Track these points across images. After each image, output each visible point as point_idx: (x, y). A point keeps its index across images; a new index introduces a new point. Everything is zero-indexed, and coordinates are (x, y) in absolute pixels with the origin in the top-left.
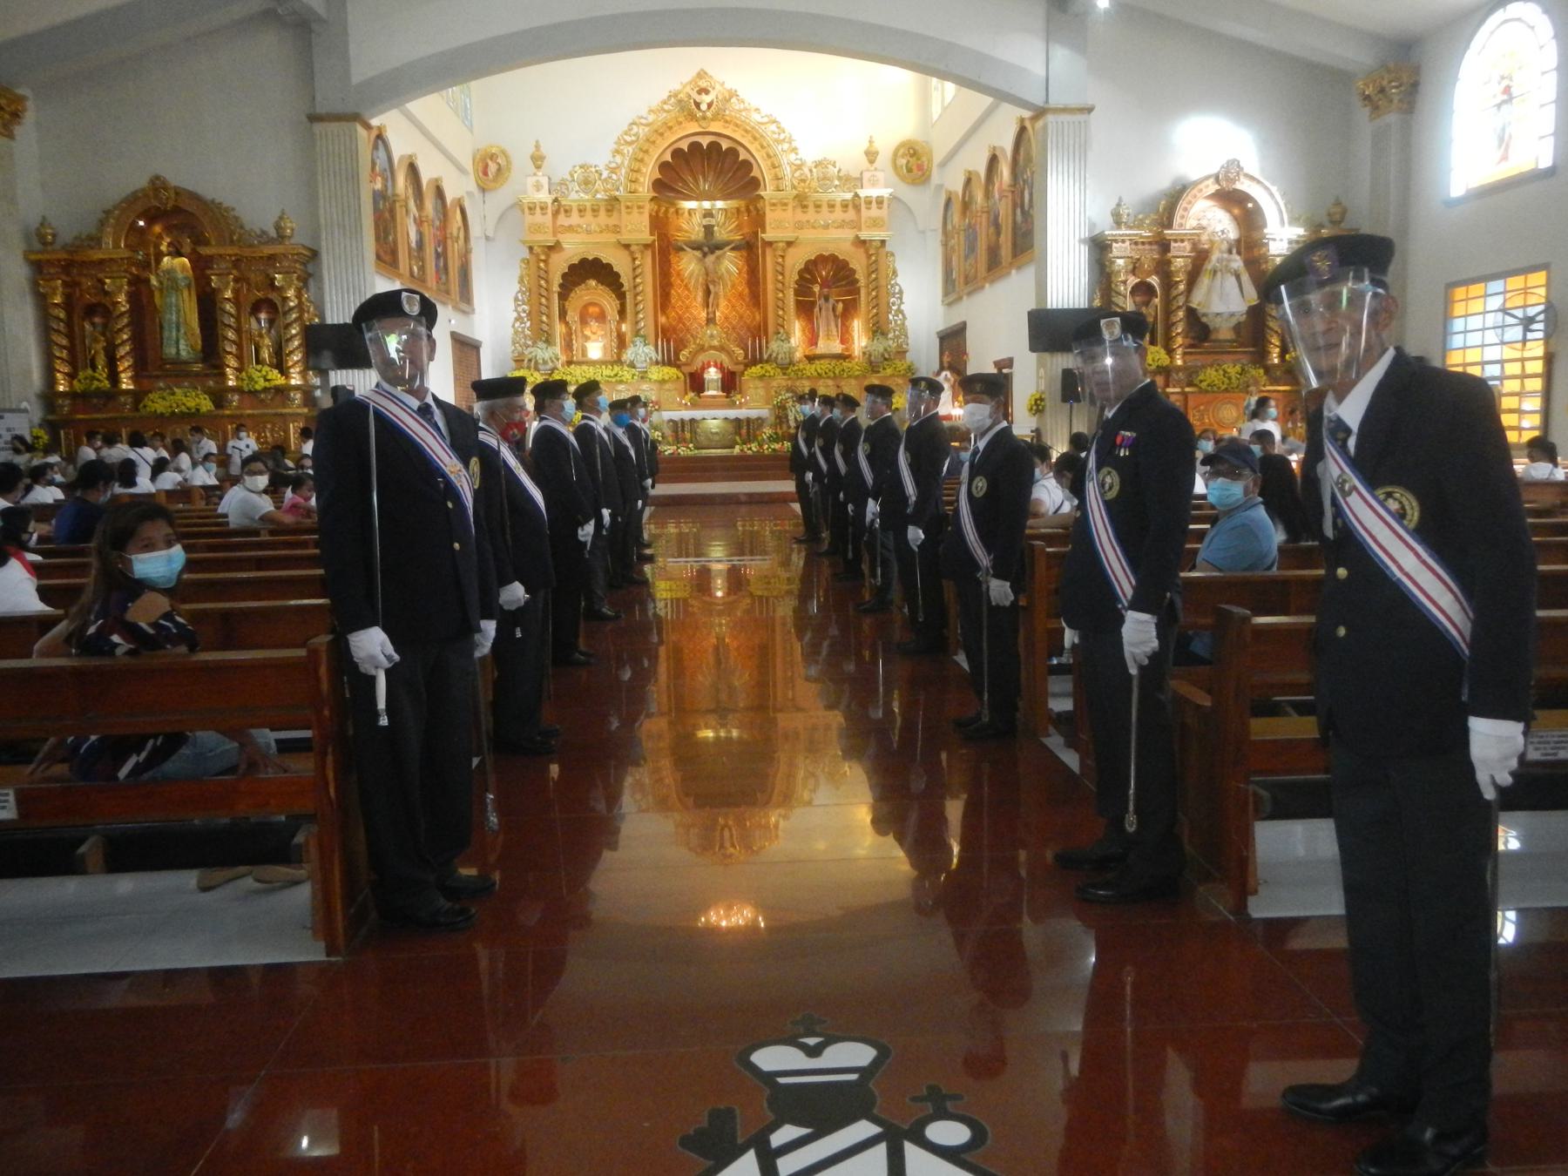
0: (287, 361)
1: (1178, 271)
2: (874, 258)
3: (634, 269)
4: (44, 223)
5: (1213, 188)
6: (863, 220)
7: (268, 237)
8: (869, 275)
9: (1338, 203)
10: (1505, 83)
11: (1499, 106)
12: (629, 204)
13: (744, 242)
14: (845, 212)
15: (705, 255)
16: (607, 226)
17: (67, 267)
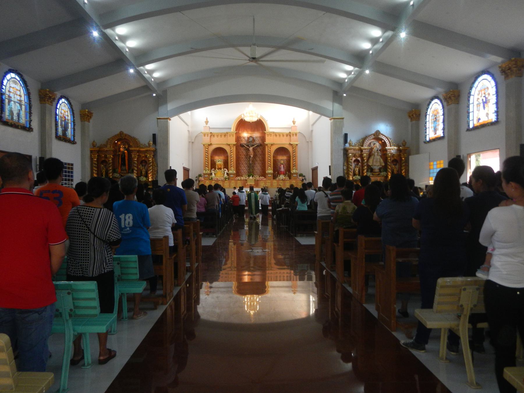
0: (149, 175)
1: (365, 157)
2: (294, 149)
3: (231, 151)
4: (94, 142)
5: (373, 137)
7: (146, 145)
8: (293, 153)
9: (404, 141)
10: (435, 117)
11: (434, 122)
13: (260, 144)
14: (287, 137)
15: (249, 147)
17: (98, 152)
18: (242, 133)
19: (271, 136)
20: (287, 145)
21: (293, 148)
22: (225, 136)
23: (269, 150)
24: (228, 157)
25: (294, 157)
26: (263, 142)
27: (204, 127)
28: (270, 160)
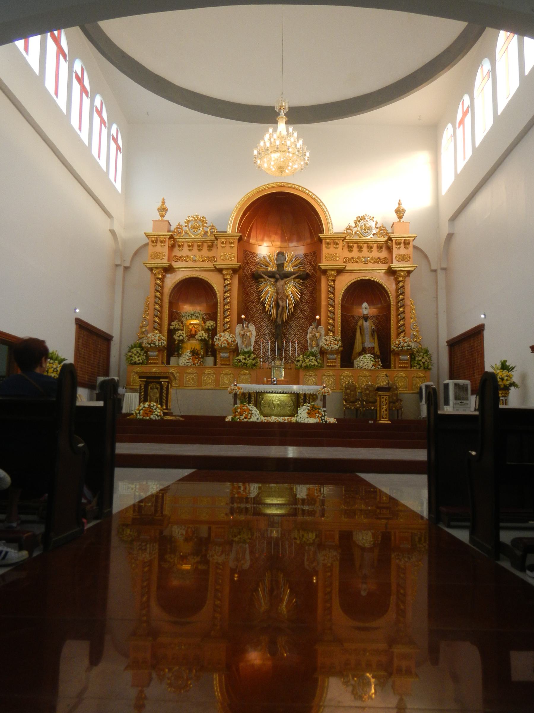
2: (401, 284)
3: (225, 287)
6: (394, 256)
8: (397, 296)
12: (223, 240)
13: (305, 273)
14: (381, 252)
15: (277, 280)
16: (208, 258)
18: (257, 245)
19: (336, 248)
20: (382, 275)
21: (400, 281)
22: (209, 246)
23: (330, 286)
24: (215, 306)
25: (401, 307)
26: (312, 266)
27: (153, 221)
28: (334, 314)
